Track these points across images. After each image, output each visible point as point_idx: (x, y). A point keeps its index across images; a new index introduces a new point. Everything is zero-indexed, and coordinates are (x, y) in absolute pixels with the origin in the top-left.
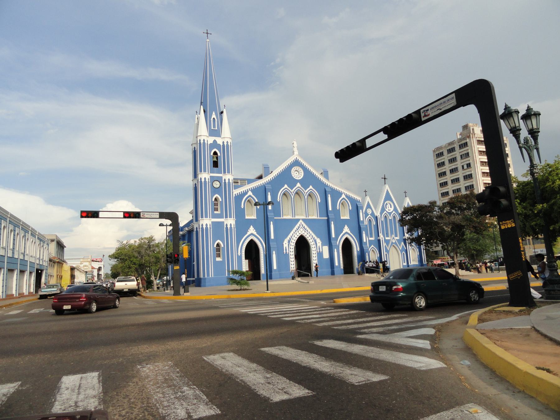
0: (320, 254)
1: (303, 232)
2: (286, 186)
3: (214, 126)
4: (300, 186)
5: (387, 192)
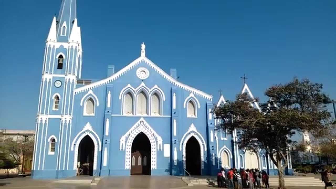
0: (160, 153)
1: (144, 129)
2: (129, 85)
3: (63, 33)
4: (144, 85)
5: (246, 89)
